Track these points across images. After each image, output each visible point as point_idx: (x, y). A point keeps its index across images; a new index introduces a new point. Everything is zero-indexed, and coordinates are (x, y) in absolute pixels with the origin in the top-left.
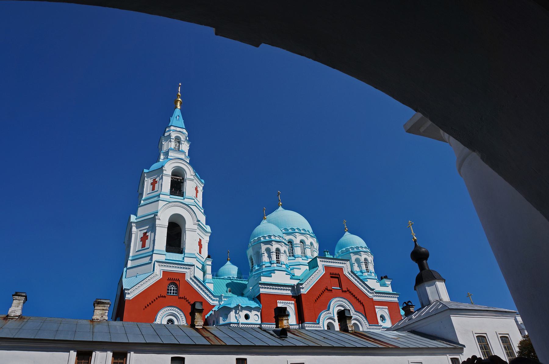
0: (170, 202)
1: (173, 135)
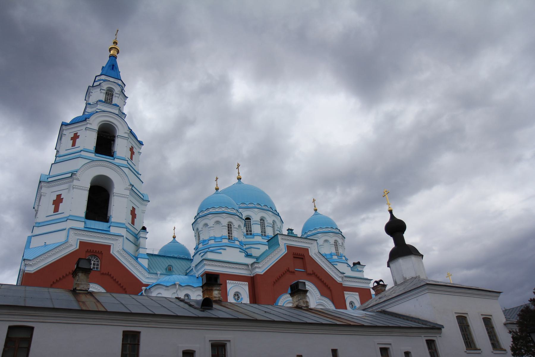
0: (93, 161)
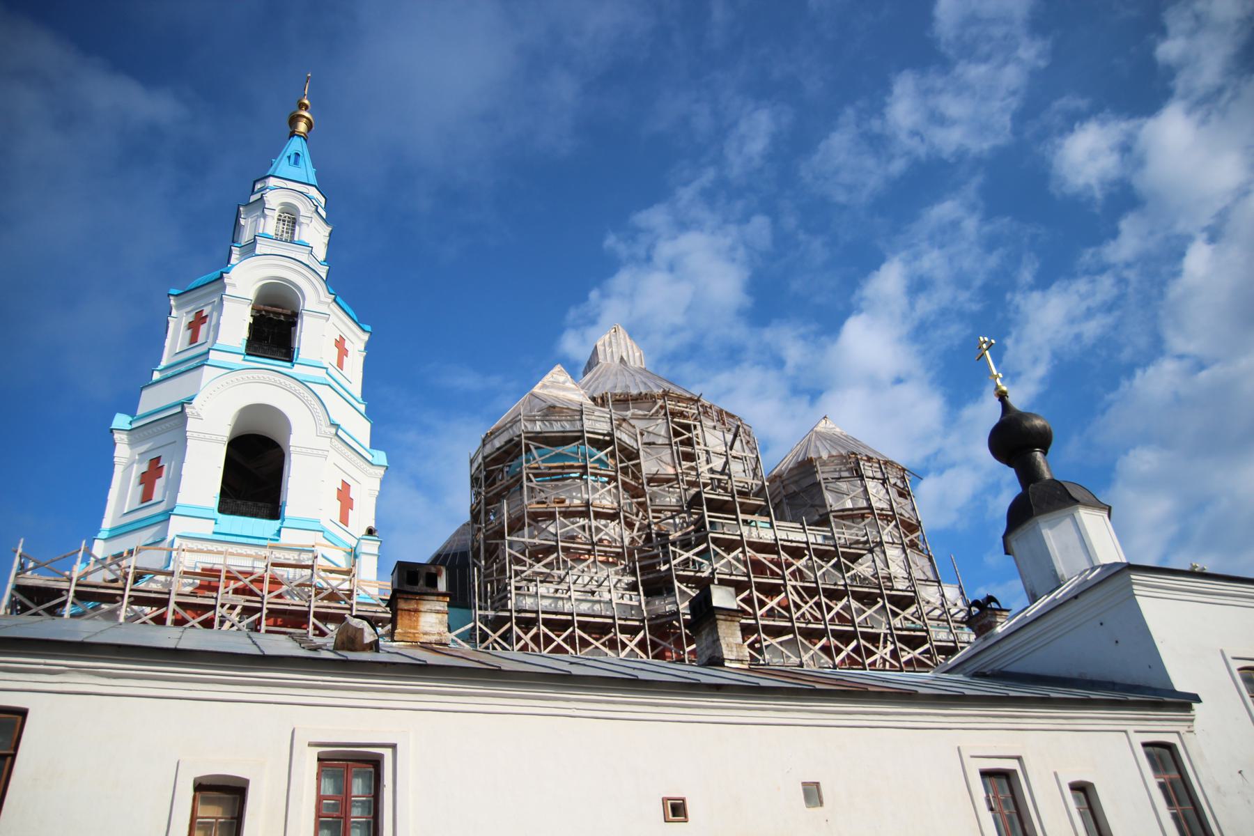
1: (274, 200)
